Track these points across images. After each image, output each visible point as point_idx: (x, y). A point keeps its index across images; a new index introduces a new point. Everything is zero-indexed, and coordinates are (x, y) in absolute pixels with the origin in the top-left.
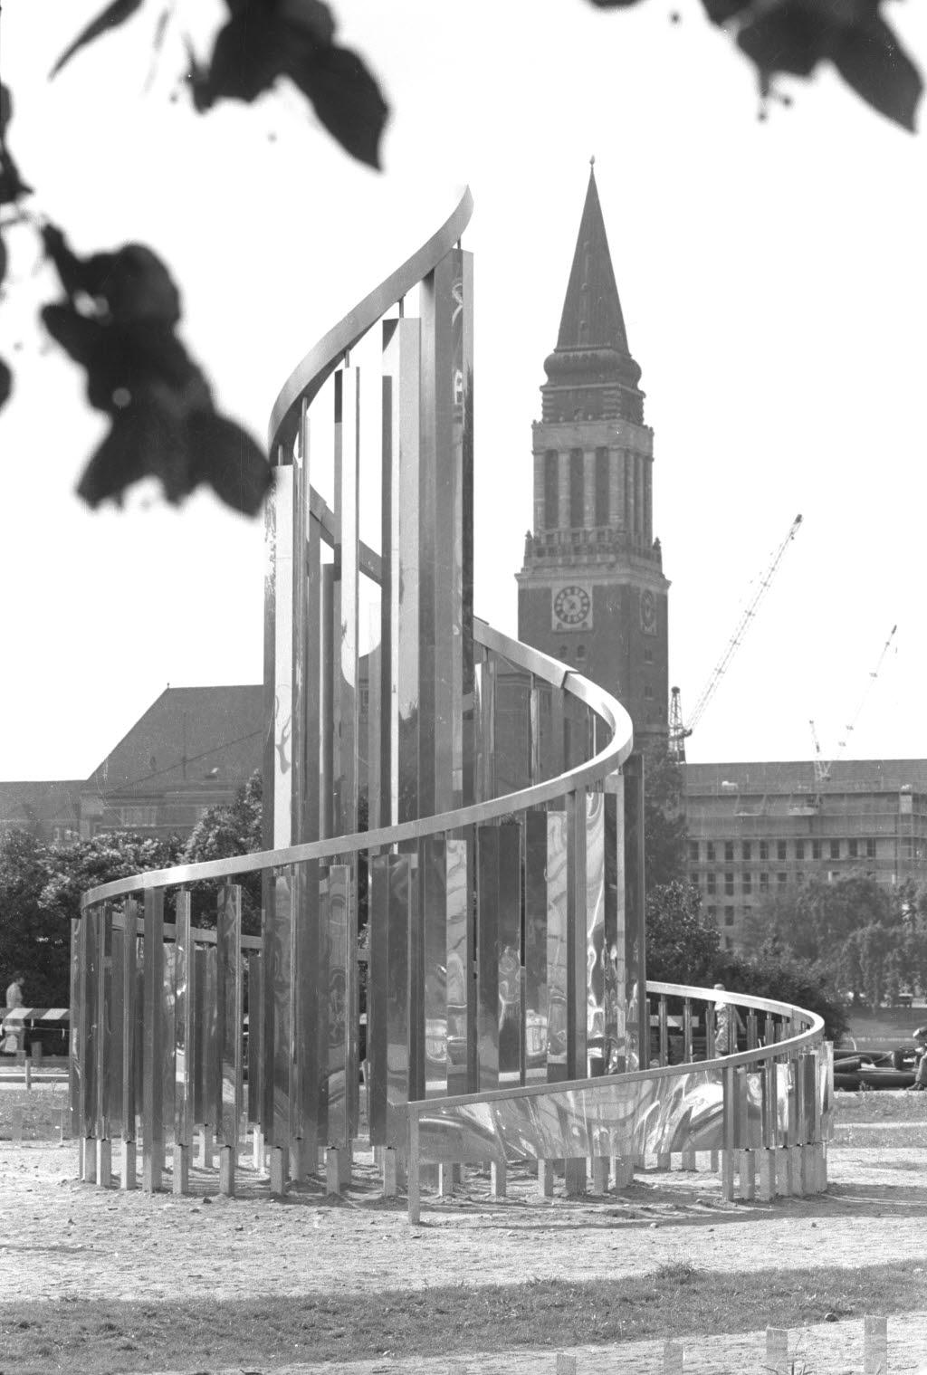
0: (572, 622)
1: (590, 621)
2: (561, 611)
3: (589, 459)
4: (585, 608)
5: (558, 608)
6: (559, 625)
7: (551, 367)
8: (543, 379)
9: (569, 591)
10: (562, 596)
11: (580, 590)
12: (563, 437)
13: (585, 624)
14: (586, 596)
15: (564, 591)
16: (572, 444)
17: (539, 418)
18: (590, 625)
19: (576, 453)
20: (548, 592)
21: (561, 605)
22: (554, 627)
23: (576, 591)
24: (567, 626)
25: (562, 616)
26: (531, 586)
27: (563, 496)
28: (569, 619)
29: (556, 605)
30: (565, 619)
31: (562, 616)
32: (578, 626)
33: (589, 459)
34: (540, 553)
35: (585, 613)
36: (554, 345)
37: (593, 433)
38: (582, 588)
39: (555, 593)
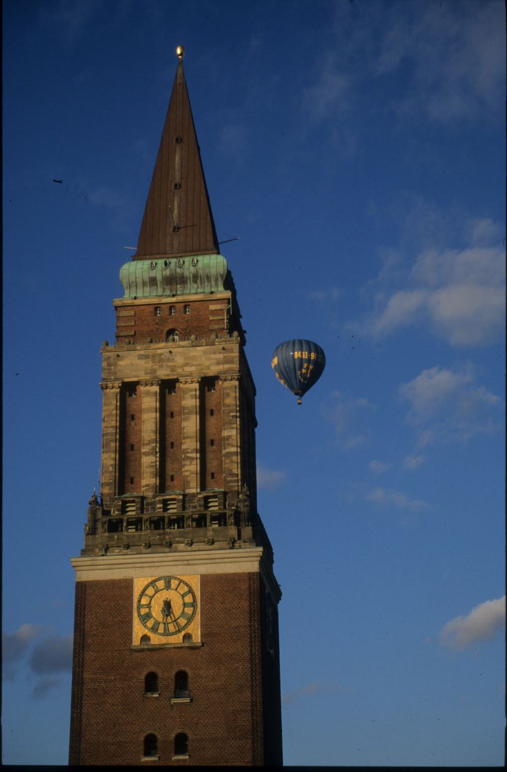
0: (167, 633)
1: (196, 631)
2: (148, 616)
4: (189, 611)
5: (143, 611)
6: (145, 638)
9: (161, 584)
10: (150, 591)
11: (181, 581)
13: (187, 637)
14: (191, 591)
15: (153, 583)
18: (197, 638)
21: (149, 606)
22: (136, 641)
23: (174, 584)
24: (156, 640)
25: (150, 624)
28: (161, 629)
29: (140, 606)
30: (154, 629)
31: (150, 624)
32: (177, 639)
35: (190, 619)
38: (184, 579)
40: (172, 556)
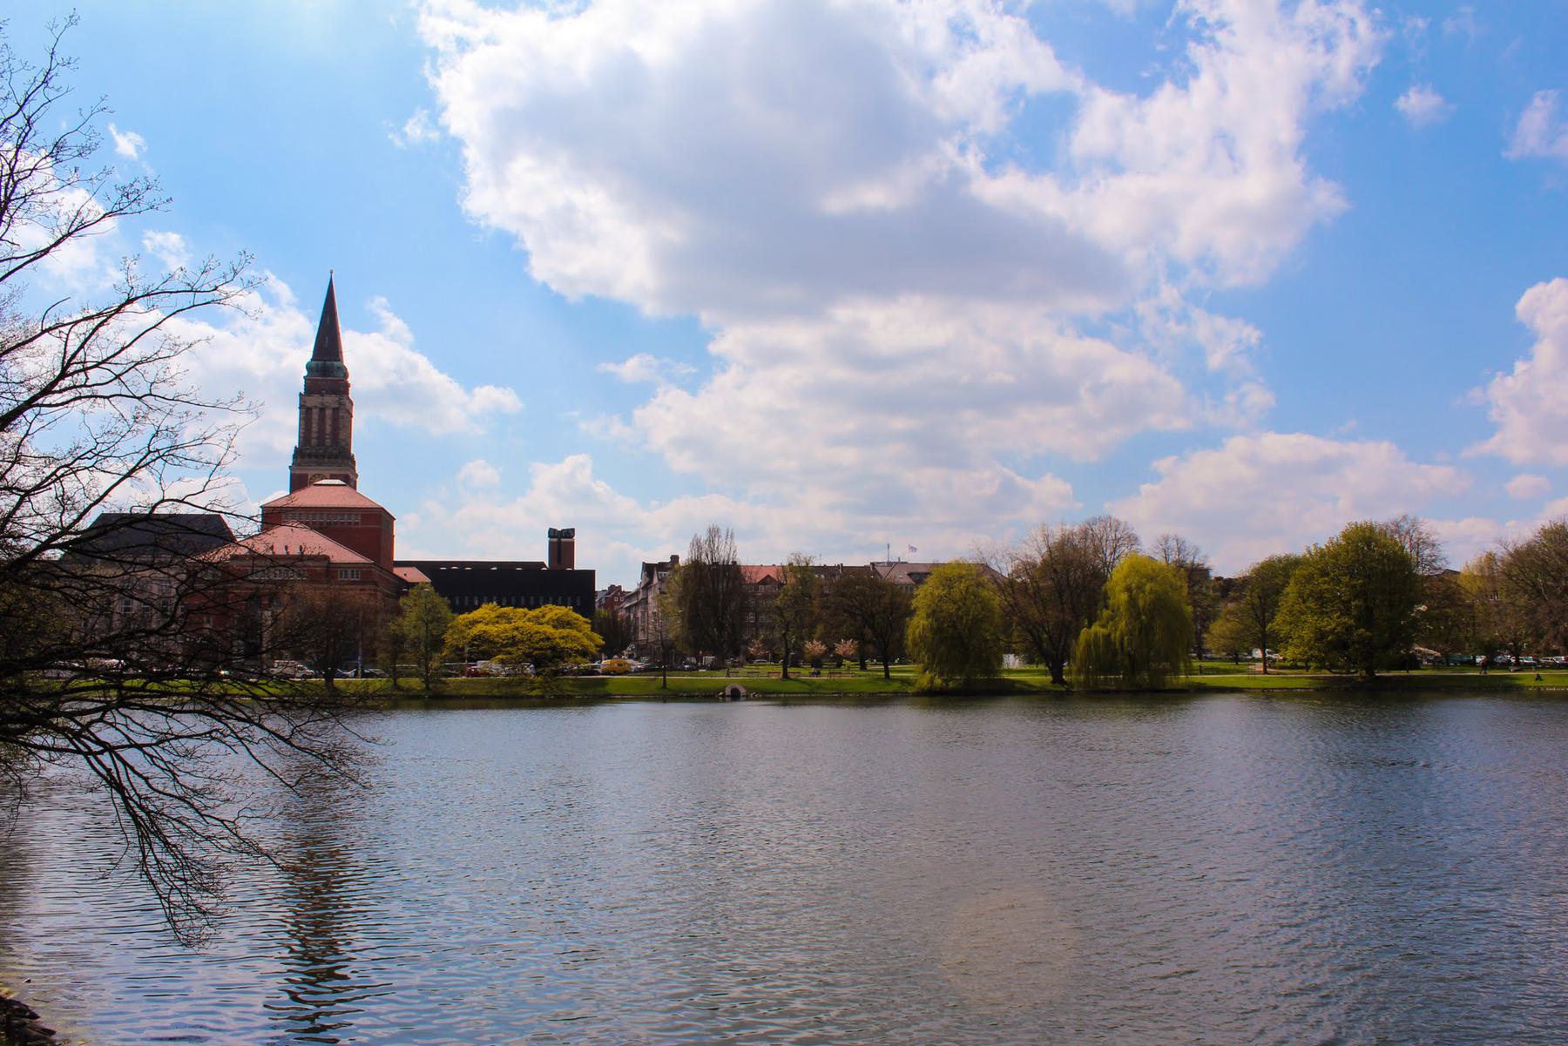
3: (329, 412)
7: (309, 367)
8: (305, 373)
12: (315, 400)
15: (314, 475)
16: (320, 406)
17: (303, 392)
19: (322, 410)
20: (307, 475)
26: (298, 472)
27: (315, 428)
33: (329, 412)
34: (302, 458)
36: (311, 357)
37: (330, 400)
39: (309, 477)
40: (321, 468)
